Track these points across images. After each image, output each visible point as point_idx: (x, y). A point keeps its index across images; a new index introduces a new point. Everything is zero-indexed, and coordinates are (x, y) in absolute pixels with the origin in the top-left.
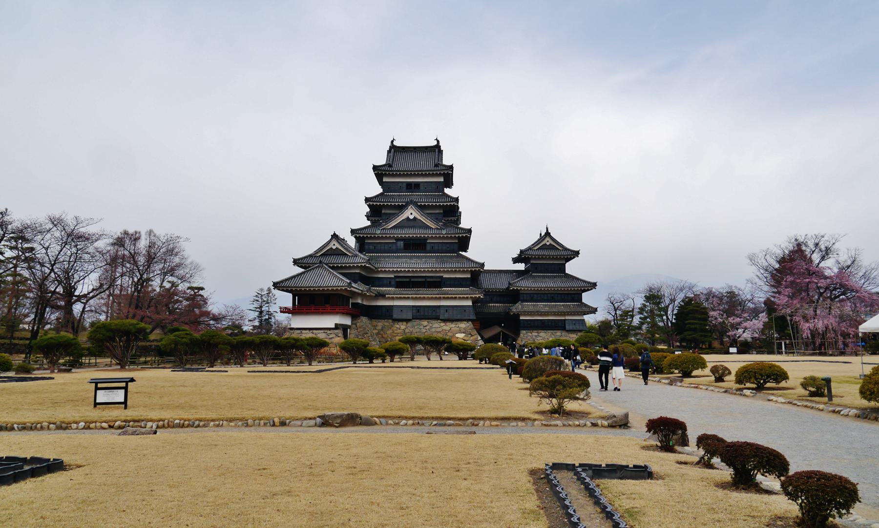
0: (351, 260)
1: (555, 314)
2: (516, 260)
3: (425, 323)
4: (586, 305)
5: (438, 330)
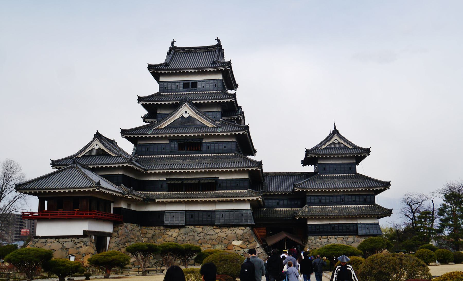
0: (112, 161)
1: (345, 218)
2: (305, 163)
3: (199, 229)
4: (380, 207)
5: (213, 237)
